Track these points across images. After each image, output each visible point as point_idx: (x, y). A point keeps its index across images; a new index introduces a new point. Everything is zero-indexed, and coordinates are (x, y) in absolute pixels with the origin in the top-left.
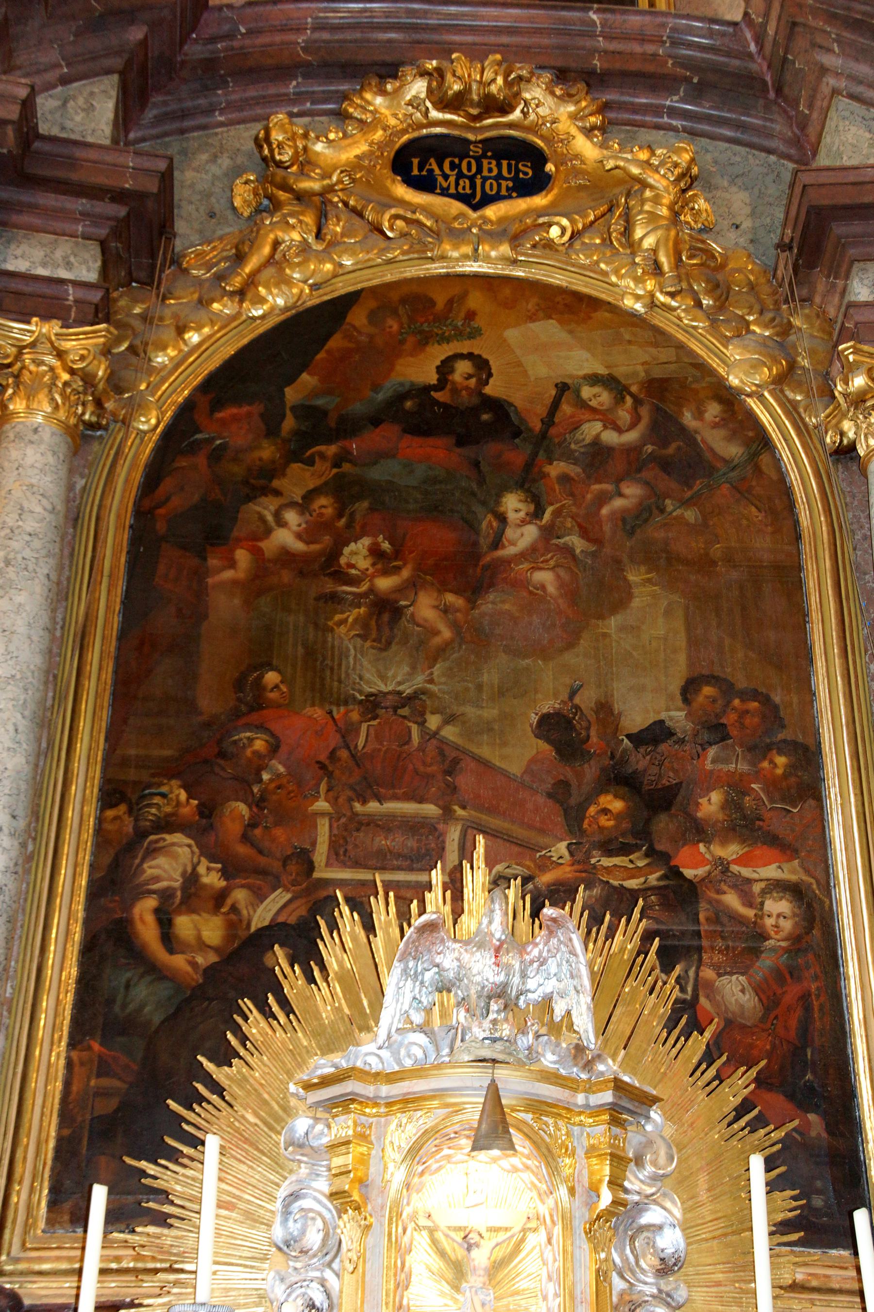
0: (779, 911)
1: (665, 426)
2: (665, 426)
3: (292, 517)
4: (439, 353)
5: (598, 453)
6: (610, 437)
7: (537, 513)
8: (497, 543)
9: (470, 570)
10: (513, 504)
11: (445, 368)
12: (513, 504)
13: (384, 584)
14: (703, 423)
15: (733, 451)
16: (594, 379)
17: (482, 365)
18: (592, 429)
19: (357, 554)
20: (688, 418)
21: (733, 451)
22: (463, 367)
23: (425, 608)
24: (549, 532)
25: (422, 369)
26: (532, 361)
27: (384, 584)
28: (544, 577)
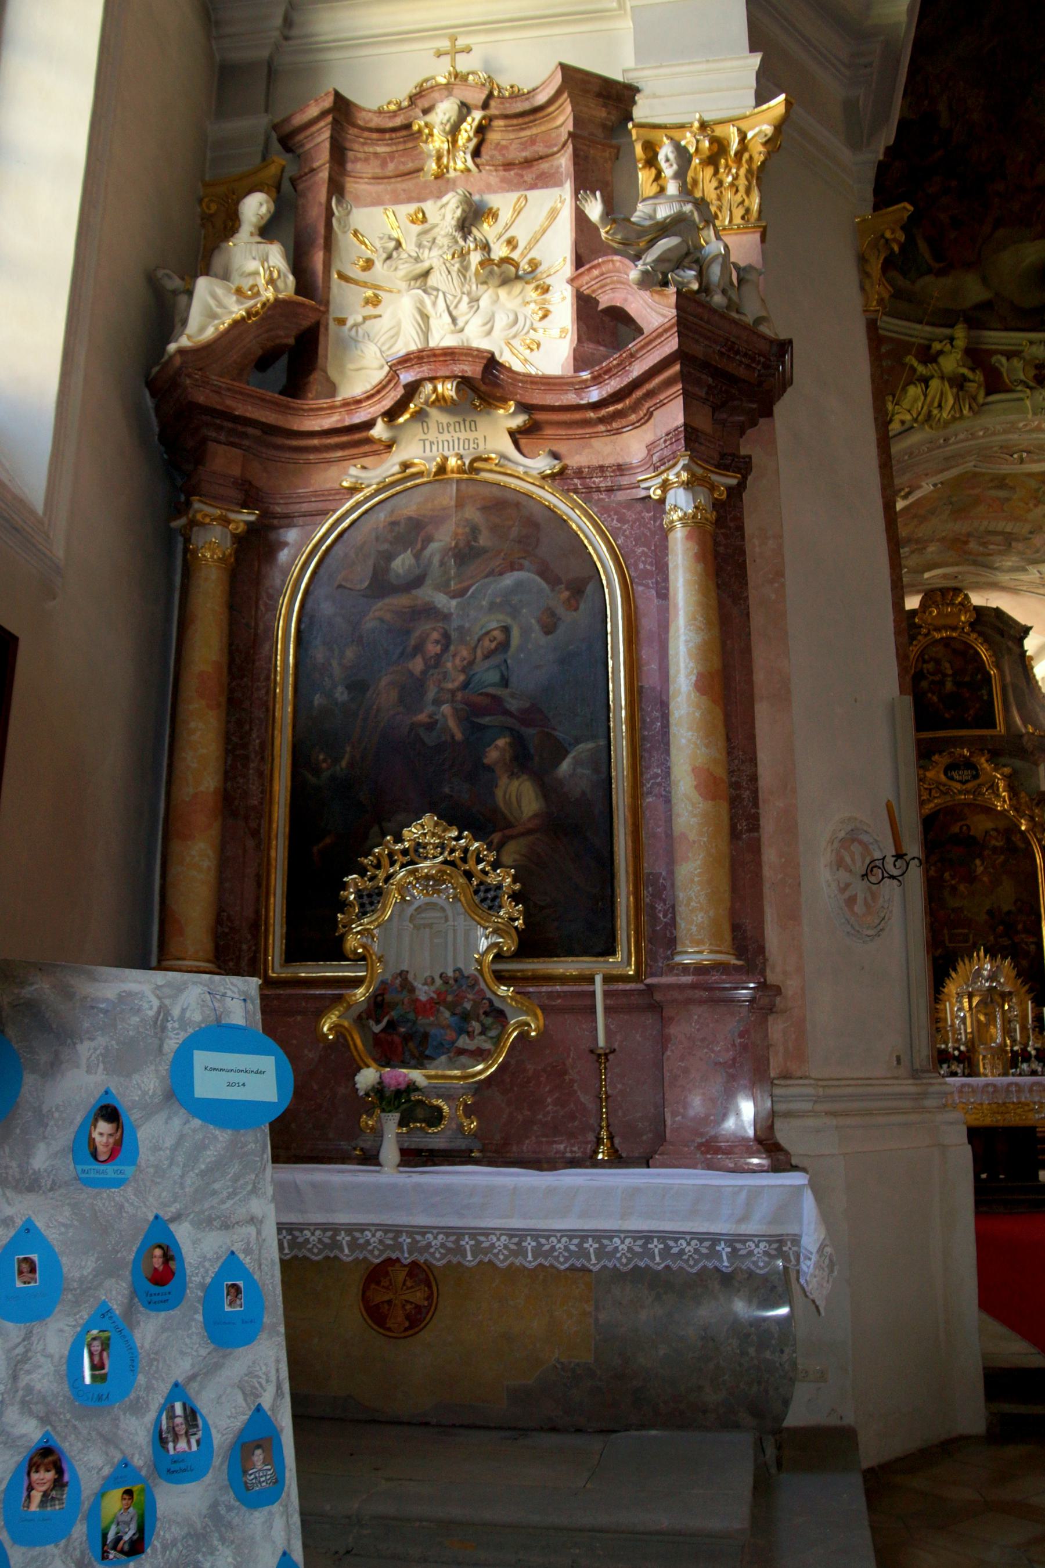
0: (1033, 947)
1: (1008, 840)
2: (1008, 840)
3: (933, 868)
4: (959, 824)
5: (995, 848)
6: (997, 844)
7: (983, 864)
8: (975, 871)
9: (971, 878)
10: (978, 862)
11: (961, 828)
12: (978, 862)
13: (953, 882)
14: (1016, 838)
15: (1023, 846)
16: (993, 829)
17: (969, 828)
18: (994, 842)
19: (947, 875)
20: (1013, 838)
21: (1023, 846)
22: (965, 828)
23: (962, 887)
24: (985, 868)
25: (956, 829)
26: (981, 825)
27: (953, 882)
28: (985, 879)
